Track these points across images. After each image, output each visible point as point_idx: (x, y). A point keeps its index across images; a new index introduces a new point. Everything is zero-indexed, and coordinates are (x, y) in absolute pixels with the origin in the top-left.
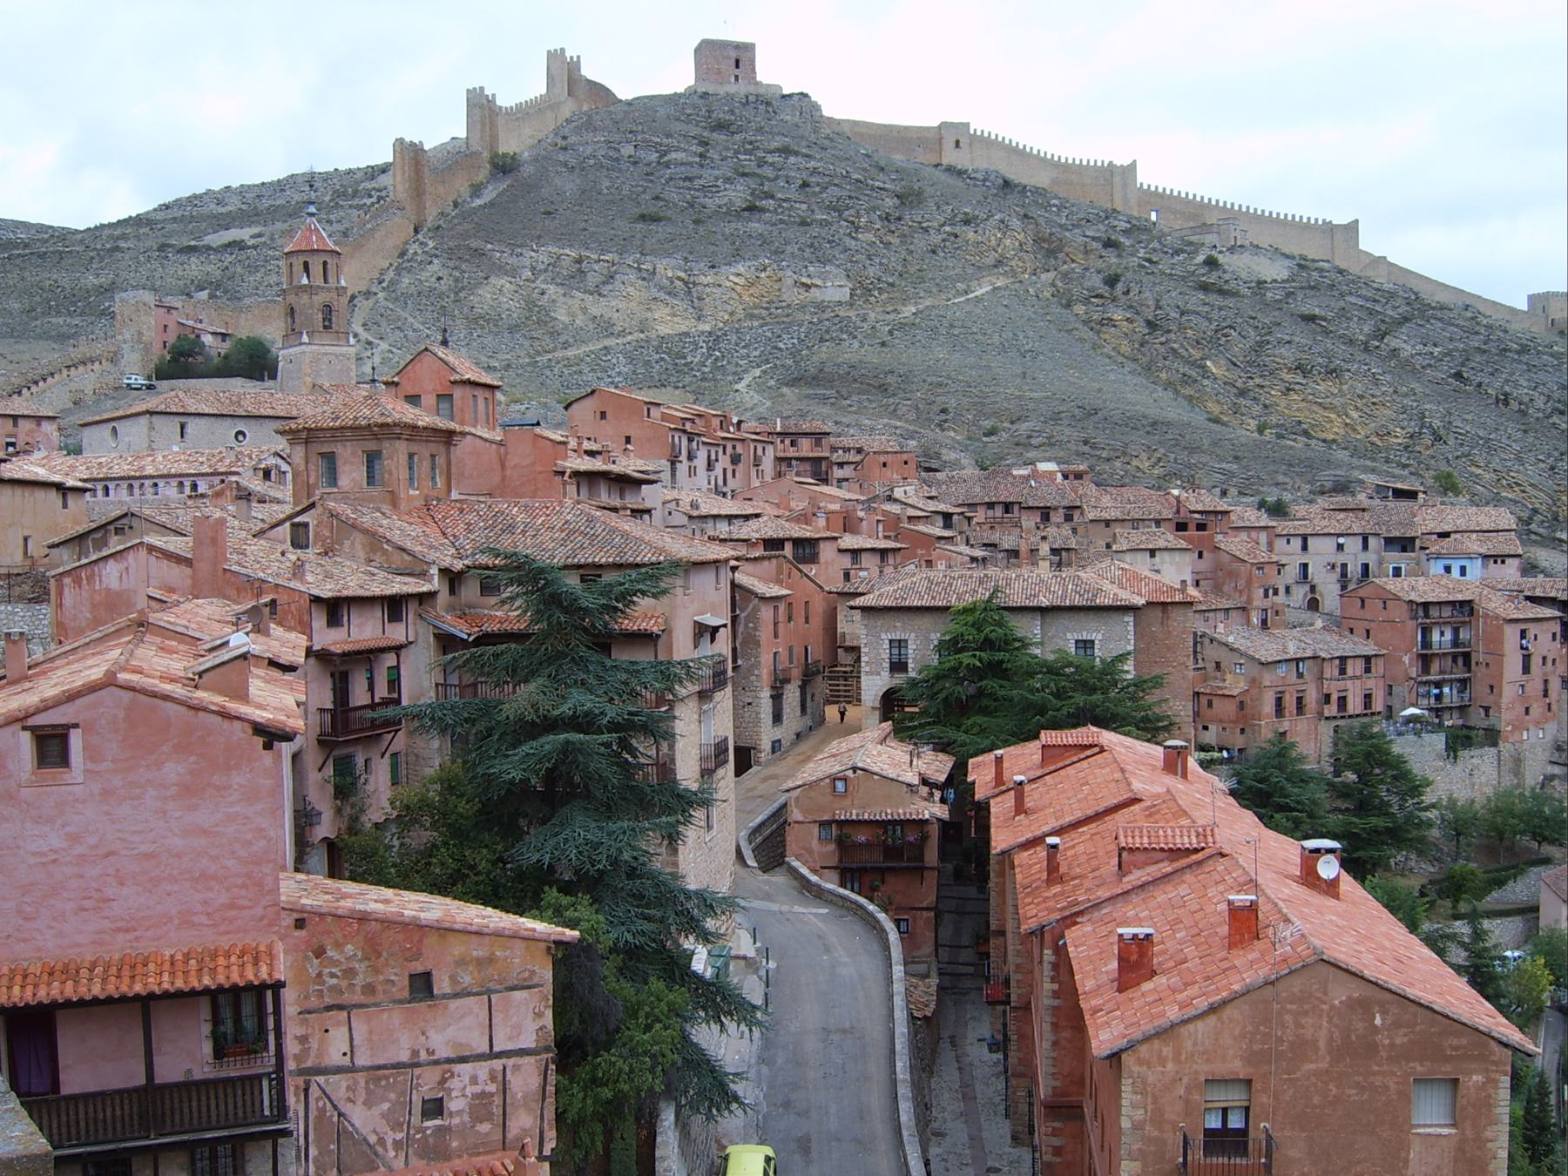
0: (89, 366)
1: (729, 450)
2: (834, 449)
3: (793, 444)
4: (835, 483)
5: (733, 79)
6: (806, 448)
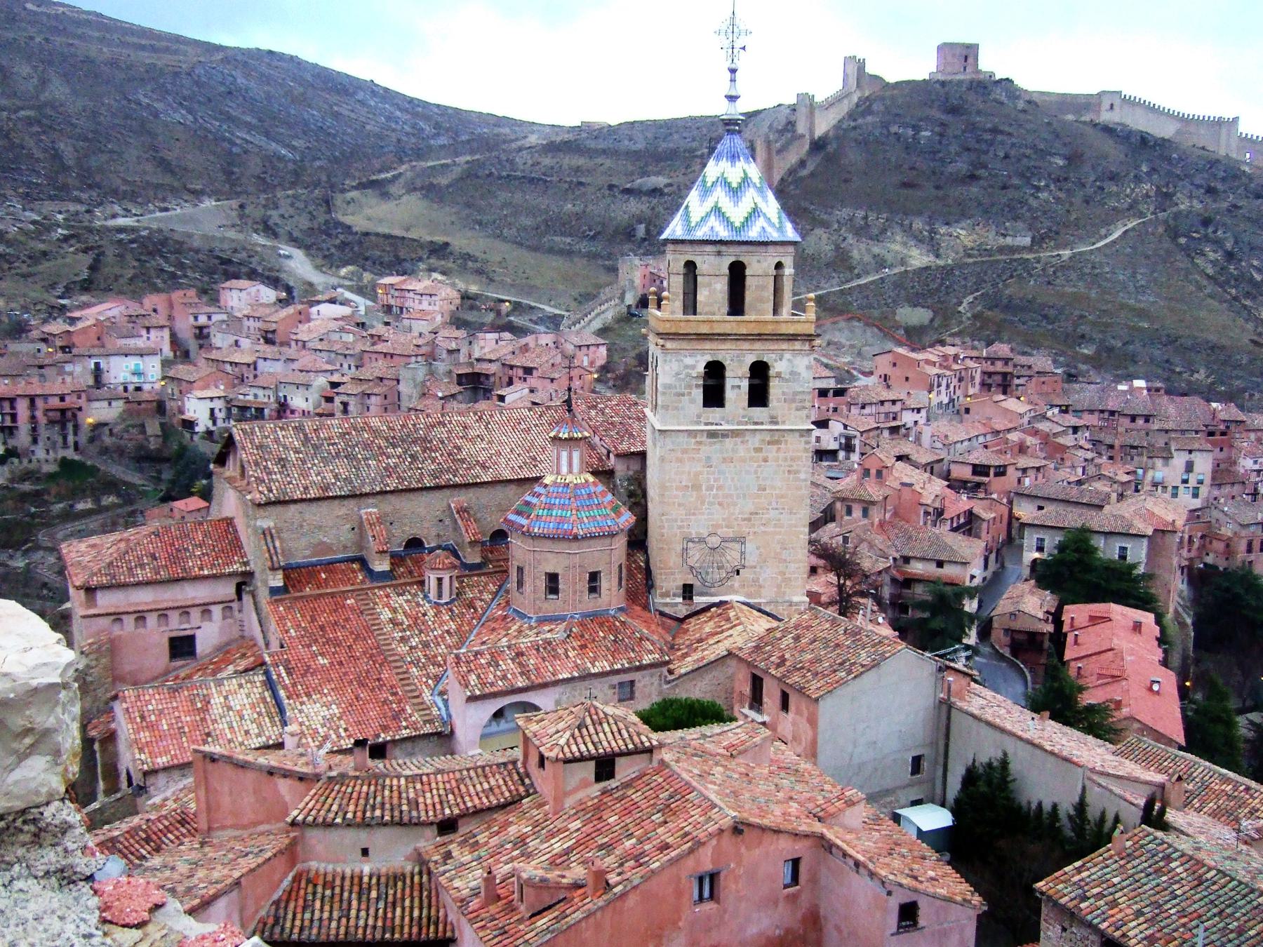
6: (999, 367)
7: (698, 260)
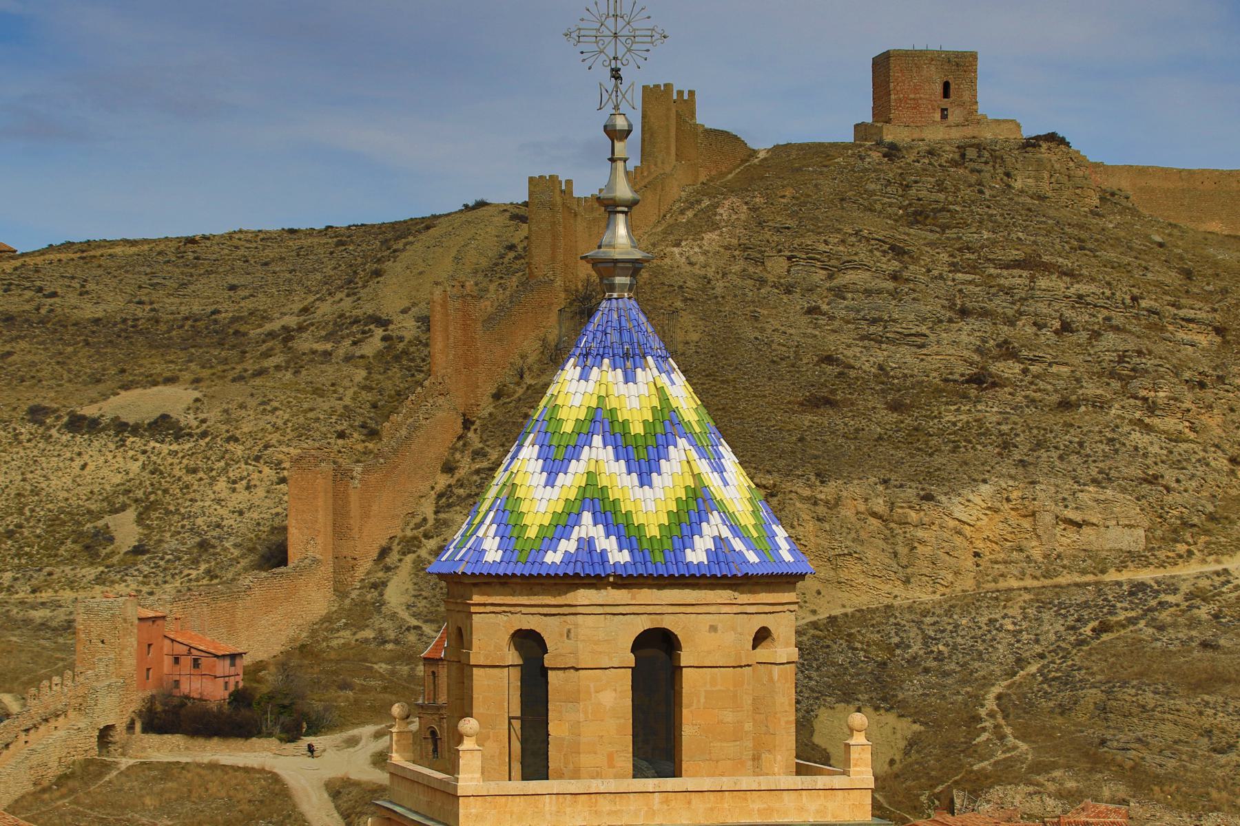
0: (52, 723)
5: (938, 116)
7: (548, 628)
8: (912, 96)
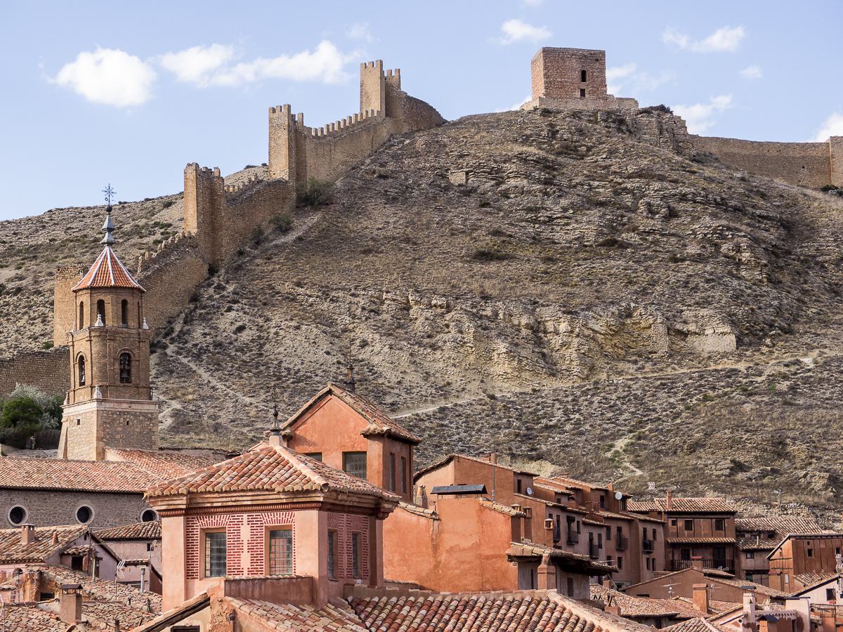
1: (614, 531)
2: (740, 532)
3: (688, 526)
4: (743, 574)
5: (578, 94)
6: (705, 533)
8: (559, 80)
